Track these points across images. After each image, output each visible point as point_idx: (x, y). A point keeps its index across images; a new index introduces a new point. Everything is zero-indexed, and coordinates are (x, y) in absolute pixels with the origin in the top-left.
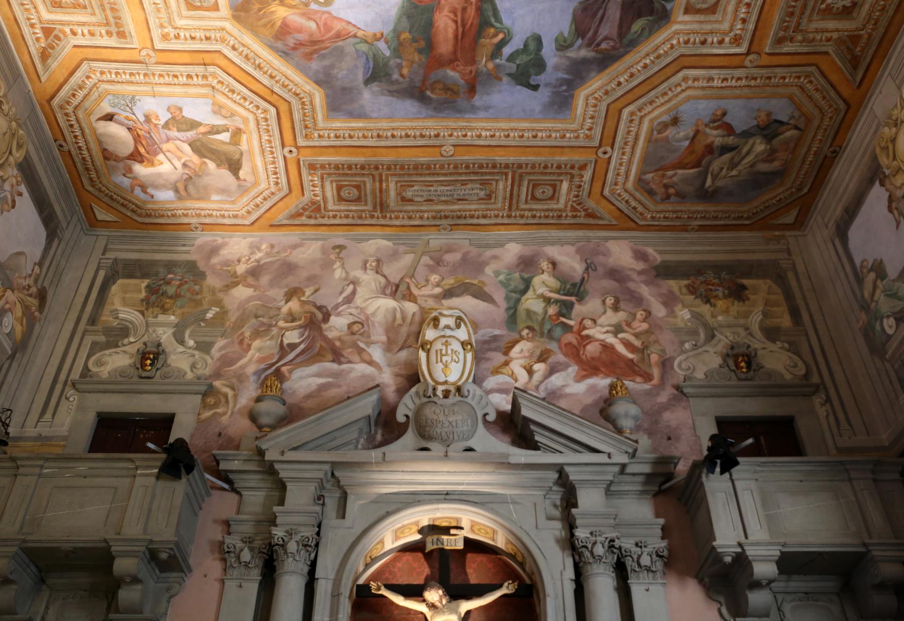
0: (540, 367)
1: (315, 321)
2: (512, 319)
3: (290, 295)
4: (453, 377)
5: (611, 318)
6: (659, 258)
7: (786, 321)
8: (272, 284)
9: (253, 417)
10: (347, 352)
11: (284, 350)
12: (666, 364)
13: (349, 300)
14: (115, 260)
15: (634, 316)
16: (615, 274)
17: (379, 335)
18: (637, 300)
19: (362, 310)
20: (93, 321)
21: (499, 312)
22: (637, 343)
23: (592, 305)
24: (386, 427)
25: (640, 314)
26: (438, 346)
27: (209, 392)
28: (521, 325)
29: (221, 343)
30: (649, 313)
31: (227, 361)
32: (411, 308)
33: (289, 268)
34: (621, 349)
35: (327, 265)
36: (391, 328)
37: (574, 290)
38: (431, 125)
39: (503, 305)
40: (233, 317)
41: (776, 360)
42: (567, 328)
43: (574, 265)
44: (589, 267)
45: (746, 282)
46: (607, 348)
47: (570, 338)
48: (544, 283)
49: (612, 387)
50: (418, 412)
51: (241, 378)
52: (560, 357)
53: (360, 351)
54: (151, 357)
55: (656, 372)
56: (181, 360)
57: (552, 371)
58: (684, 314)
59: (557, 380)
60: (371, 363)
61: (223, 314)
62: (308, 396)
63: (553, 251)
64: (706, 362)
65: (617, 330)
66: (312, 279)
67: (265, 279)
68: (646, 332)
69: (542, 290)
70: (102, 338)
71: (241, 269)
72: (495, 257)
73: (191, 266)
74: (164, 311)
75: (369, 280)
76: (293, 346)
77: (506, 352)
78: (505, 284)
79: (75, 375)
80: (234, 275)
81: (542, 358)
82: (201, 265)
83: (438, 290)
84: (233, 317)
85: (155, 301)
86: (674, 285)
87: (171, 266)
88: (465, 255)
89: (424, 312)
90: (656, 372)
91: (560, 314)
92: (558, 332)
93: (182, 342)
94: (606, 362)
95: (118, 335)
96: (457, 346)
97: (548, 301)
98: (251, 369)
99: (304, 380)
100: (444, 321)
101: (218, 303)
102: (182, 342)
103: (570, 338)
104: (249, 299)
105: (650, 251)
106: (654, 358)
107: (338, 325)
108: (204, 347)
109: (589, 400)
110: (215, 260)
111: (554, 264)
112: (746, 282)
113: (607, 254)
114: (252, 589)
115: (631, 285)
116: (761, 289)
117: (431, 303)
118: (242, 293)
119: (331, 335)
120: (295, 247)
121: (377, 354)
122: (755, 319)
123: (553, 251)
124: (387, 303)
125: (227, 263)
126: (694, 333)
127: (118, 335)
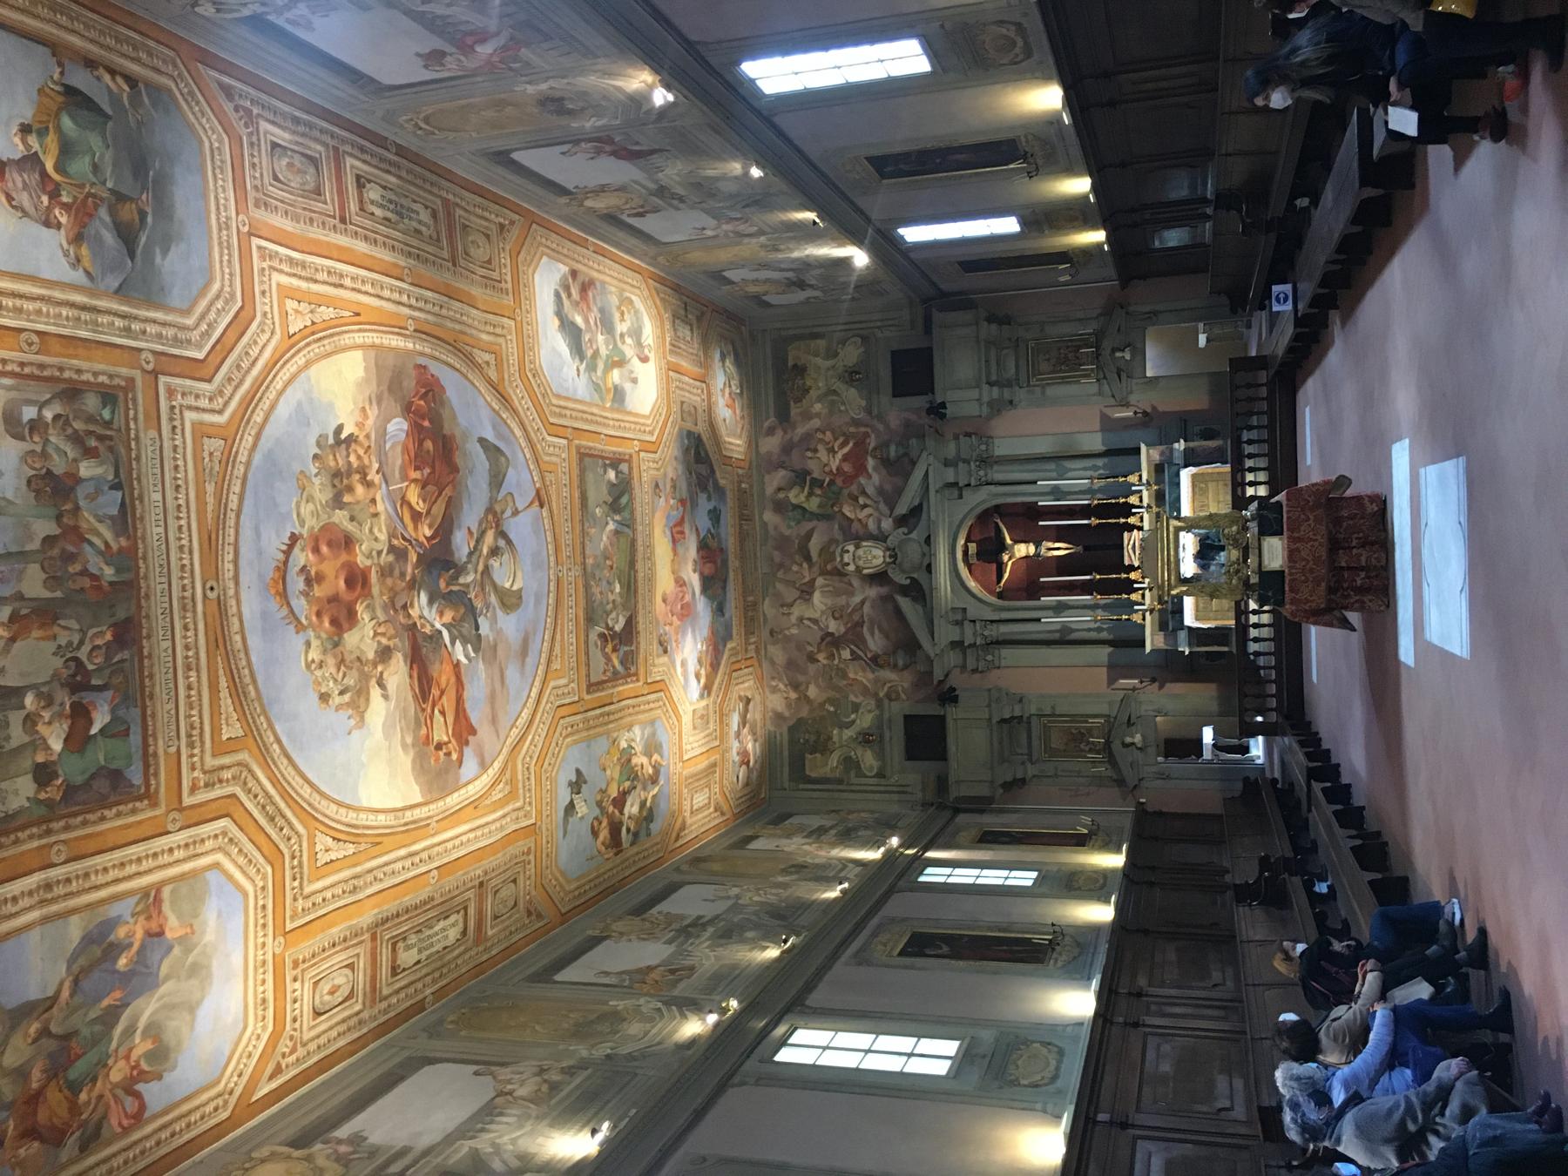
0: (861, 501)
1: (832, 642)
2: (827, 517)
3: (812, 659)
4: (879, 553)
5: (823, 454)
6: (772, 420)
7: (822, 343)
8: (805, 673)
9: (906, 667)
10: (856, 617)
11: (855, 657)
12: (856, 423)
13: (815, 621)
14: (790, 780)
15: (821, 440)
16: (787, 449)
17: (842, 600)
18: (808, 437)
19: (823, 612)
20: (840, 781)
21: (821, 526)
22: (841, 440)
23: (812, 465)
24: (919, 591)
25: (820, 436)
26: (861, 563)
27: (888, 696)
28: (829, 511)
29: (852, 698)
30: (818, 430)
31: (866, 691)
32: (820, 581)
33: (791, 665)
34: (846, 450)
35: (788, 639)
36: (837, 593)
37: (801, 477)
38: (731, 575)
39: (815, 523)
40: (831, 694)
41: (851, 354)
42: (832, 482)
43: (780, 476)
44: (782, 465)
45: (790, 364)
46: (845, 458)
47: (839, 482)
48: (796, 496)
49: (874, 457)
50: (903, 571)
51: (876, 681)
52: (854, 488)
53: (854, 610)
54: (865, 739)
55: (863, 429)
56: (865, 720)
57: (864, 493)
58: (818, 407)
59: (870, 490)
60: (863, 602)
61: (830, 701)
62: (887, 637)
63: (769, 490)
64: (853, 398)
65: (832, 451)
66: (799, 647)
67: (801, 678)
68: (833, 432)
69: (802, 498)
70: (853, 774)
71: (793, 695)
72: (776, 528)
73: (790, 729)
74: (830, 738)
75: (797, 611)
76: (853, 653)
77: (851, 521)
78: (799, 523)
79: (883, 781)
80: (798, 699)
81: (856, 499)
82: (791, 723)
83: (805, 565)
84: (831, 694)
85: (822, 746)
86: (795, 411)
87: (792, 742)
88: (777, 548)
89: (823, 573)
90: (863, 429)
91: (821, 486)
92: (834, 488)
93: (853, 722)
94: (856, 460)
95: (850, 763)
96: (860, 552)
97: (811, 494)
98: (871, 676)
99: (875, 643)
100: (846, 560)
101: (822, 705)
102: (853, 722)
103: (839, 482)
104: (818, 686)
105: (766, 424)
106: (852, 429)
107: (833, 626)
108: (856, 708)
109: (884, 472)
110: (787, 714)
111: (780, 489)
112: (790, 364)
113: (769, 453)
114: (1006, 652)
115: (796, 439)
116: (794, 354)
117: (816, 569)
118: (812, 692)
119: (843, 630)
120: (773, 663)
121: (857, 599)
122: (819, 360)
123: (769, 490)
124: (817, 596)
125: (789, 706)
126: (833, 403)
127: (850, 763)
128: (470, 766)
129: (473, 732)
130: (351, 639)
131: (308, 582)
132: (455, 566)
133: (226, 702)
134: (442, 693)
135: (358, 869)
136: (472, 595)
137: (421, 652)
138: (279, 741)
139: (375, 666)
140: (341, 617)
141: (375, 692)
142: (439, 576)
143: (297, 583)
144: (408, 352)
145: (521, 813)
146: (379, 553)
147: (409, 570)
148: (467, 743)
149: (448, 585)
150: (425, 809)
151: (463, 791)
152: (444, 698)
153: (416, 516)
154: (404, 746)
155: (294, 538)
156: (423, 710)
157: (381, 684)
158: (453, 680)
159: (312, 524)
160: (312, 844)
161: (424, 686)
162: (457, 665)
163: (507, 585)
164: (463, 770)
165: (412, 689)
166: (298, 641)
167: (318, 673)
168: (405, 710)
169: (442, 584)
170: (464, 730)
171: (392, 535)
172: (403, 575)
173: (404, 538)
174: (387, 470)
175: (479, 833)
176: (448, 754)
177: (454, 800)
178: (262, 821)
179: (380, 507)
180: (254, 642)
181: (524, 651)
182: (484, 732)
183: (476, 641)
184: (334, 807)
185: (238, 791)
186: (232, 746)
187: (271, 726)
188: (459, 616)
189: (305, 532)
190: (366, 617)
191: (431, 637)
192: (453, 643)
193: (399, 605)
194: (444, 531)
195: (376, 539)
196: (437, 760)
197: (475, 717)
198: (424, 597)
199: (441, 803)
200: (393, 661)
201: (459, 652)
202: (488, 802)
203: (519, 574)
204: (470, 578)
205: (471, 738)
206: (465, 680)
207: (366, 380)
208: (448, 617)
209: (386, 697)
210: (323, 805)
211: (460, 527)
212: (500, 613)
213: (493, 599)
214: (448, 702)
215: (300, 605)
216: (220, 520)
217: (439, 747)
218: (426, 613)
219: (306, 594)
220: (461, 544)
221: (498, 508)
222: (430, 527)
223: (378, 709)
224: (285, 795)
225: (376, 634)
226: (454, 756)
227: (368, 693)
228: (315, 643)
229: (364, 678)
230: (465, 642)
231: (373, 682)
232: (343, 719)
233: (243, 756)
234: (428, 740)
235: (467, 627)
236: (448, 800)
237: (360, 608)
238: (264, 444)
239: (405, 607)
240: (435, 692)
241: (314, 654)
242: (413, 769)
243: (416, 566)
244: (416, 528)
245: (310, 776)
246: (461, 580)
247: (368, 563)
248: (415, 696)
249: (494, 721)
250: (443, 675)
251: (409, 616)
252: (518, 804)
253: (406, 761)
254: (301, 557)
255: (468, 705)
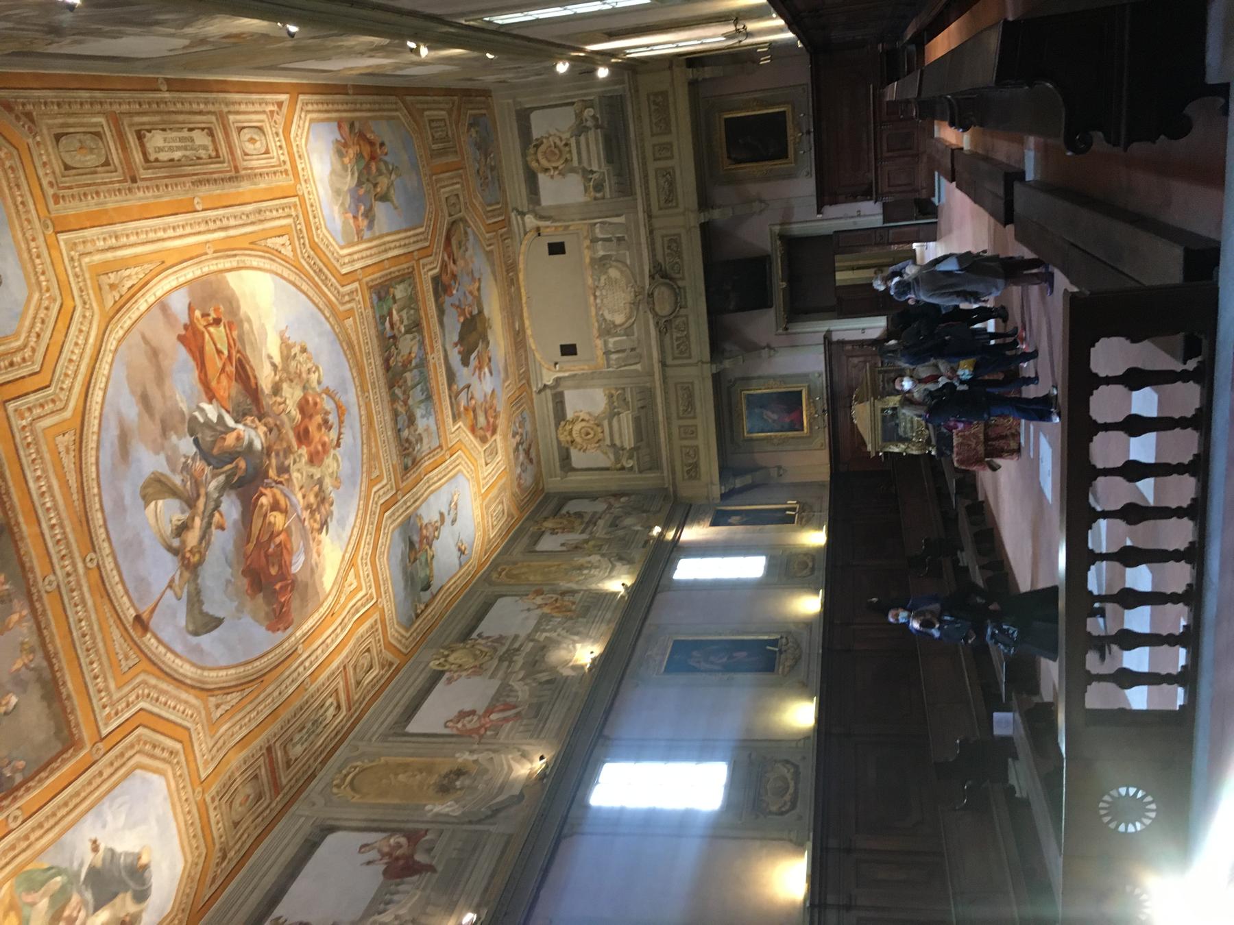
128: (179, 304)
129: (181, 339)
130: (299, 394)
131: (326, 422)
132: (232, 487)
133: (354, 338)
134: (223, 370)
135: (261, 227)
136: (208, 470)
137: (251, 400)
138: (327, 319)
139: (281, 379)
140: (305, 407)
141: (277, 359)
142: (247, 469)
143: (332, 418)
144: (299, 626)
145: (81, 248)
146: (295, 462)
147: (274, 461)
148: (186, 327)
149: (237, 467)
150: (221, 267)
151: (182, 280)
152: (220, 365)
153: (275, 506)
154: (249, 320)
155: (338, 445)
156: (238, 352)
157: (274, 366)
158: (214, 384)
159: (329, 461)
160: (294, 250)
161: (243, 374)
162: (211, 396)
163: (160, 502)
164: (186, 301)
165: (251, 367)
166: (327, 382)
167: (310, 365)
168: (254, 349)
169: (242, 464)
170: (192, 339)
171: (289, 480)
172: (277, 455)
173: (281, 483)
174: (300, 525)
175: (152, 236)
176: (205, 315)
177: (190, 272)
178: (325, 270)
179: (300, 496)
180: (348, 375)
181: (124, 440)
182: (168, 340)
183: (194, 428)
184: (285, 275)
185: (341, 289)
186: (350, 313)
187: (332, 327)
188: (218, 445)
189: (332, 452)
190: (293, 413)
191: (244, 415)
192: (220, 417)
193: (275, 431)
194: (249, 507)
195: (298, 470)
196: (216, 310)
197: (182, 353)
198: (258, 445)
199: (206, 270)
200: (270, 386)
201: (211, 411)
202: (148, 267)
203: (152, 521)
204: (213, 484)
205: (183, 332)
206: (199, 387)
207: (321, 576)
208: (230, 439)
209: (270, 357)
210: (293, 277)
211: (235, 522)
212: (164, 468)
213: (177, 480)
214: (215, 364)
215: (328, 405)
216: (369, 438)
217: (217, 322)
218: (253, 433)
219: (327, 413)
220: (231, 509)
221: (187, 575)
222: (262, 505)
223: (273, 348)
224: (316, 285)
225: (284, 402)
226: (198, 313)
227: (282, 357)
228: (315, 384)
229: (286, 369)
230: (208, 424)
231: (280, 367)
232: (294, 337)
233: (342, 308)
234: (230, 326)
235: (207, 437)
236: (198, 273)
237: (299, 417)
238: (358, 490)
239: (270, 430)
240: (231, 369)
241: (314, 377)
242: (238, 301)
243: (269, 466)
244: (274, 496)
245: (304, 297)
246: (222, 478)
247: (300, 451)
248: (248, 362)
249: (154, 354)
250: (227, 387)
251: (265, 425)
252: (87, 260)
253: (245, 308)
254: (333, 434)
255: (192, 363)
